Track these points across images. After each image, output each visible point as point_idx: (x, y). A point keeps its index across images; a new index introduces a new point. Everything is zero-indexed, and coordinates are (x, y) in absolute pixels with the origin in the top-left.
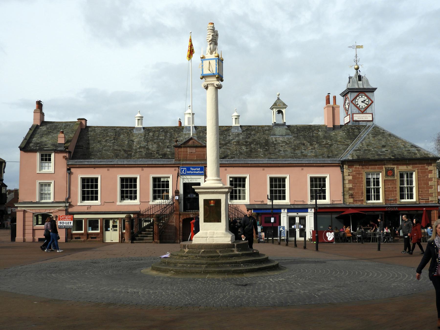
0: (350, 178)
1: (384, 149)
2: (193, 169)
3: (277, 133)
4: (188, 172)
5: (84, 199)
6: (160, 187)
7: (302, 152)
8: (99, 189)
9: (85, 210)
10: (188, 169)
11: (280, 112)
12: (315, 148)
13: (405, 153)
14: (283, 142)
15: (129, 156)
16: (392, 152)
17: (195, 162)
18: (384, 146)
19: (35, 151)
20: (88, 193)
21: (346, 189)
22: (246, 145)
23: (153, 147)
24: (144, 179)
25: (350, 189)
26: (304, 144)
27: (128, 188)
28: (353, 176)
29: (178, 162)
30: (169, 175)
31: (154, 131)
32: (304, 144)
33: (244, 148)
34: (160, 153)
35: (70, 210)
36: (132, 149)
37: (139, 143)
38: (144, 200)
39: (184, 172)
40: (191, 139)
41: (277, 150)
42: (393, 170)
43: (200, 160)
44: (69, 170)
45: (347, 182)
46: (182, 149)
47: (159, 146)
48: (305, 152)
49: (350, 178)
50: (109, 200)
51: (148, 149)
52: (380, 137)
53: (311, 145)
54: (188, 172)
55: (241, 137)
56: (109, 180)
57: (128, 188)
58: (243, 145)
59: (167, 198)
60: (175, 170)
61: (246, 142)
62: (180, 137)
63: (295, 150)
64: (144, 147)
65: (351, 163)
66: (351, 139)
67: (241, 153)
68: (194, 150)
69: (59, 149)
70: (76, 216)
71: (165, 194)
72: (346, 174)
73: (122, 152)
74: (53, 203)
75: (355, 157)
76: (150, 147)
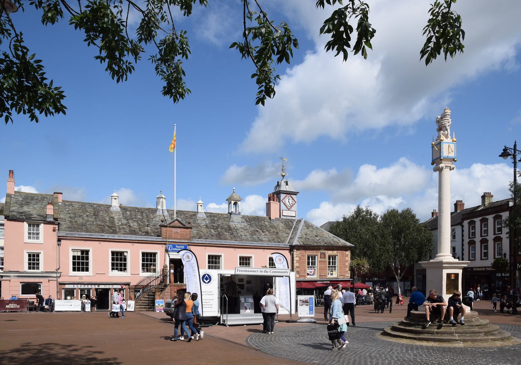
0: (298, 259)
1: (317, 238)
2: (178, 247)
3: (235, 220)
4: (174, 249)
5: (74, 269)
6: (149, 260)
7: (258, 237)
8: (141, 262)
9: (77, 280)
10: (174, 247)
11: (235, 204)
12: (266, 235)
13: (332, 242)
14: (242, 228)
15: (115, 232)
16: (323, 241)
17: (178, 241)
18: (316, 236)
19: (23, 221)
20: (117, 264)
21: (295, 267)
22: (214, 229)
23: (134, 225)
24: (134, 254)
25: (297, 267)
26: (258, 231)
27: (119, 261)
28: (300, 257)
29: (165, 240)
30: (159, 250)
31: (130, 211)
32: (258, 231)
33: (212, 231)
34: (143, 231)
35: (60, 280)
36: (115, 225)
37: (120, 220)
38: (134, 273)
39: (171, 249)
40: (177, 220)
41: (239, 235)
42: (324, 254)
43: (184, 239)
44: (59, 240)
45: (295, 262)
46: (168, 229)
47: (139, 225)
48: (261, 237)
49: (298, 259)
50: (100, 271)
51: (130, 226)
52: (311, 229)
53: (263, 232)
54: (174, 249)
55: (207, 222)
56: (100, 254)
57: (119, 261)
58: (212, 228)
59: (155, 271)
60: (162, 247)
61: (213, 226)
62: (155, 217)
63: (252, 235)
64: (126, 225)
65: (299, 248)
66: (289, 229)
67: (212, 236)
68: (179, 230)
69: (48, 220)
70: (67, 286)
71: (152, 267)
72: (295, 256)
73: (107, 228)
74: (42, 273)
75: (302, 244)
76: (132, 225)
